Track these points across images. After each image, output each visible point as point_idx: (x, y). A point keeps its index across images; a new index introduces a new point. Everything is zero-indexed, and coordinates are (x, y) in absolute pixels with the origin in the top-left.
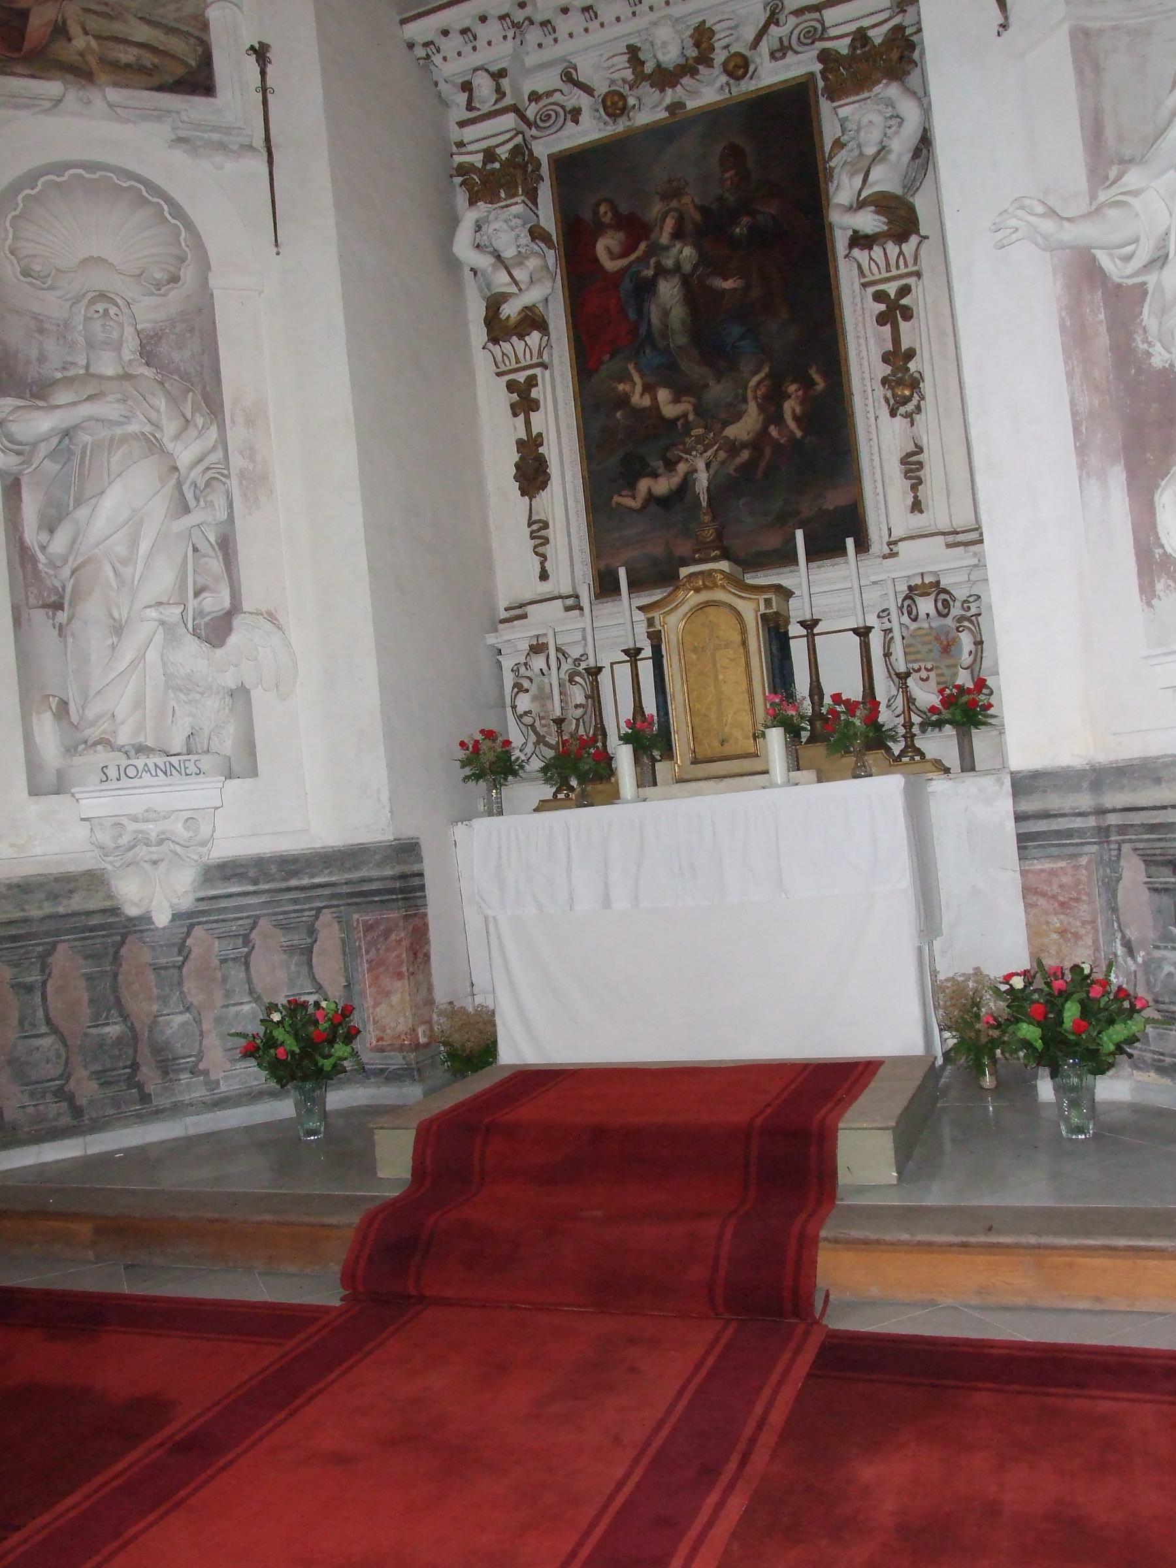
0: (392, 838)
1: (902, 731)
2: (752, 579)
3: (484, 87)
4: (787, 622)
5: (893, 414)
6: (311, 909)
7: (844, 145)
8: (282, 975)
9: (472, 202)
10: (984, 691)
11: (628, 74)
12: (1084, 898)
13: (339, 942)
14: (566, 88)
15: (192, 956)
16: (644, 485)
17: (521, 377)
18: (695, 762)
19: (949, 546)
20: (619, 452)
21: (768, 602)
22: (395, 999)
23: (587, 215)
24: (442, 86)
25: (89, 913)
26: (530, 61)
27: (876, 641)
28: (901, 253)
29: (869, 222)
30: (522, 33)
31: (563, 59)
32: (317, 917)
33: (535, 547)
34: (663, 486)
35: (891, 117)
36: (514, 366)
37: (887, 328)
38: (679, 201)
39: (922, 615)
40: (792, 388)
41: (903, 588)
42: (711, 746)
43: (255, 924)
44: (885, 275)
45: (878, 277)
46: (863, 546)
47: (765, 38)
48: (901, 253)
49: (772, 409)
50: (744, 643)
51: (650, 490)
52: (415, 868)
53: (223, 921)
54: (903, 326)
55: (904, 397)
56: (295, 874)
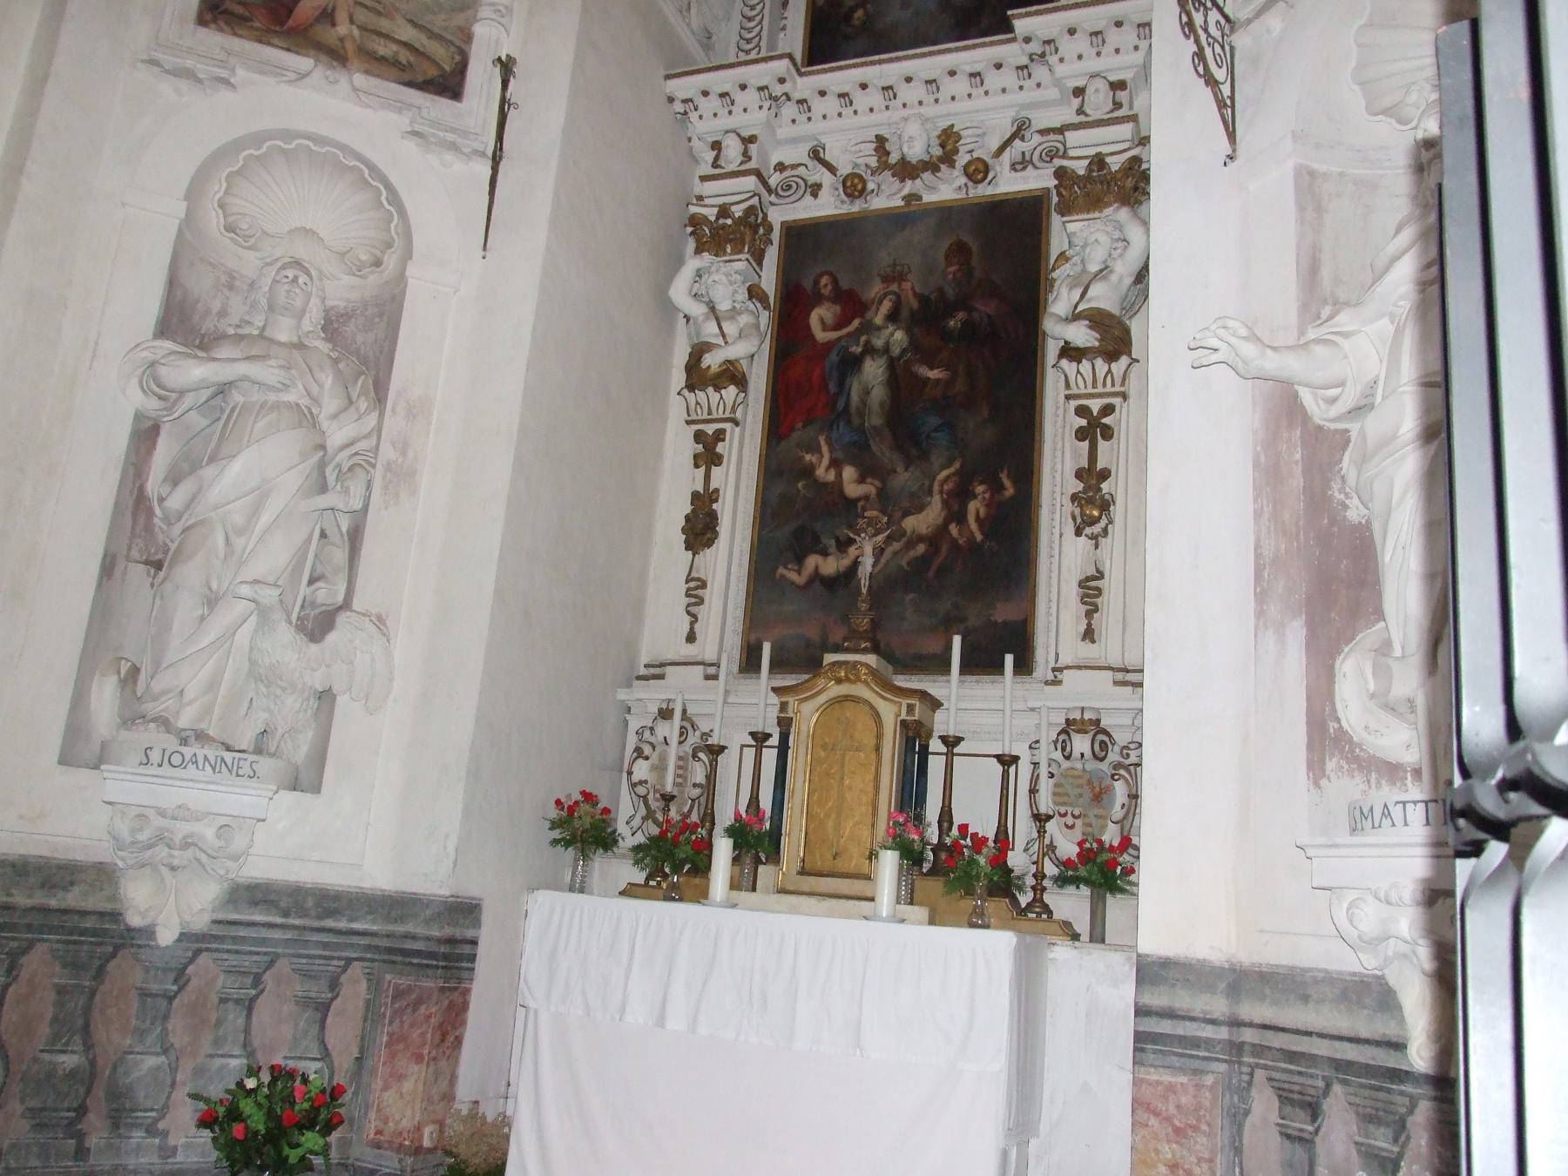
0: (447, 893)
1: (1030, 881)
2: (902, 681)
3: (733, 148)
4: (930, 735)
5: (1078, 533)
6: (339, 958)
7: (1067, 259)
8: (287, 1030)
9: (698, 251)
10: (1131, 851)
12: (1204, 1127)
13: (361, 1004)
14: (810, 163)
15: (190, 987)
16: (812, 561)
17: (710, 429)
18: (803, 872)
19: (1116, 683)
20: (795, 521)
21: (910, 708)
22: (408, 1086)
23: (808, 284)
24: (695, 143)
25: (84, 913)
26: (782, 133)
27: (1024, 768)
28: (1109, 371)
29: (1081, 335)
30: (779, 107)
32: (344, 970)
34: (831, 566)
36: (706, 416)
39: (1076, 754)
40: (980, 489)
42: (822, 860)
43: (272, 963)
46: (1024, 666)
48: (1109, 371)
50: (878, 749)
52: (470, 934)
53: (237, 952)
54: (1102, 445)
55: (1091, 516)
56: (330, 913)
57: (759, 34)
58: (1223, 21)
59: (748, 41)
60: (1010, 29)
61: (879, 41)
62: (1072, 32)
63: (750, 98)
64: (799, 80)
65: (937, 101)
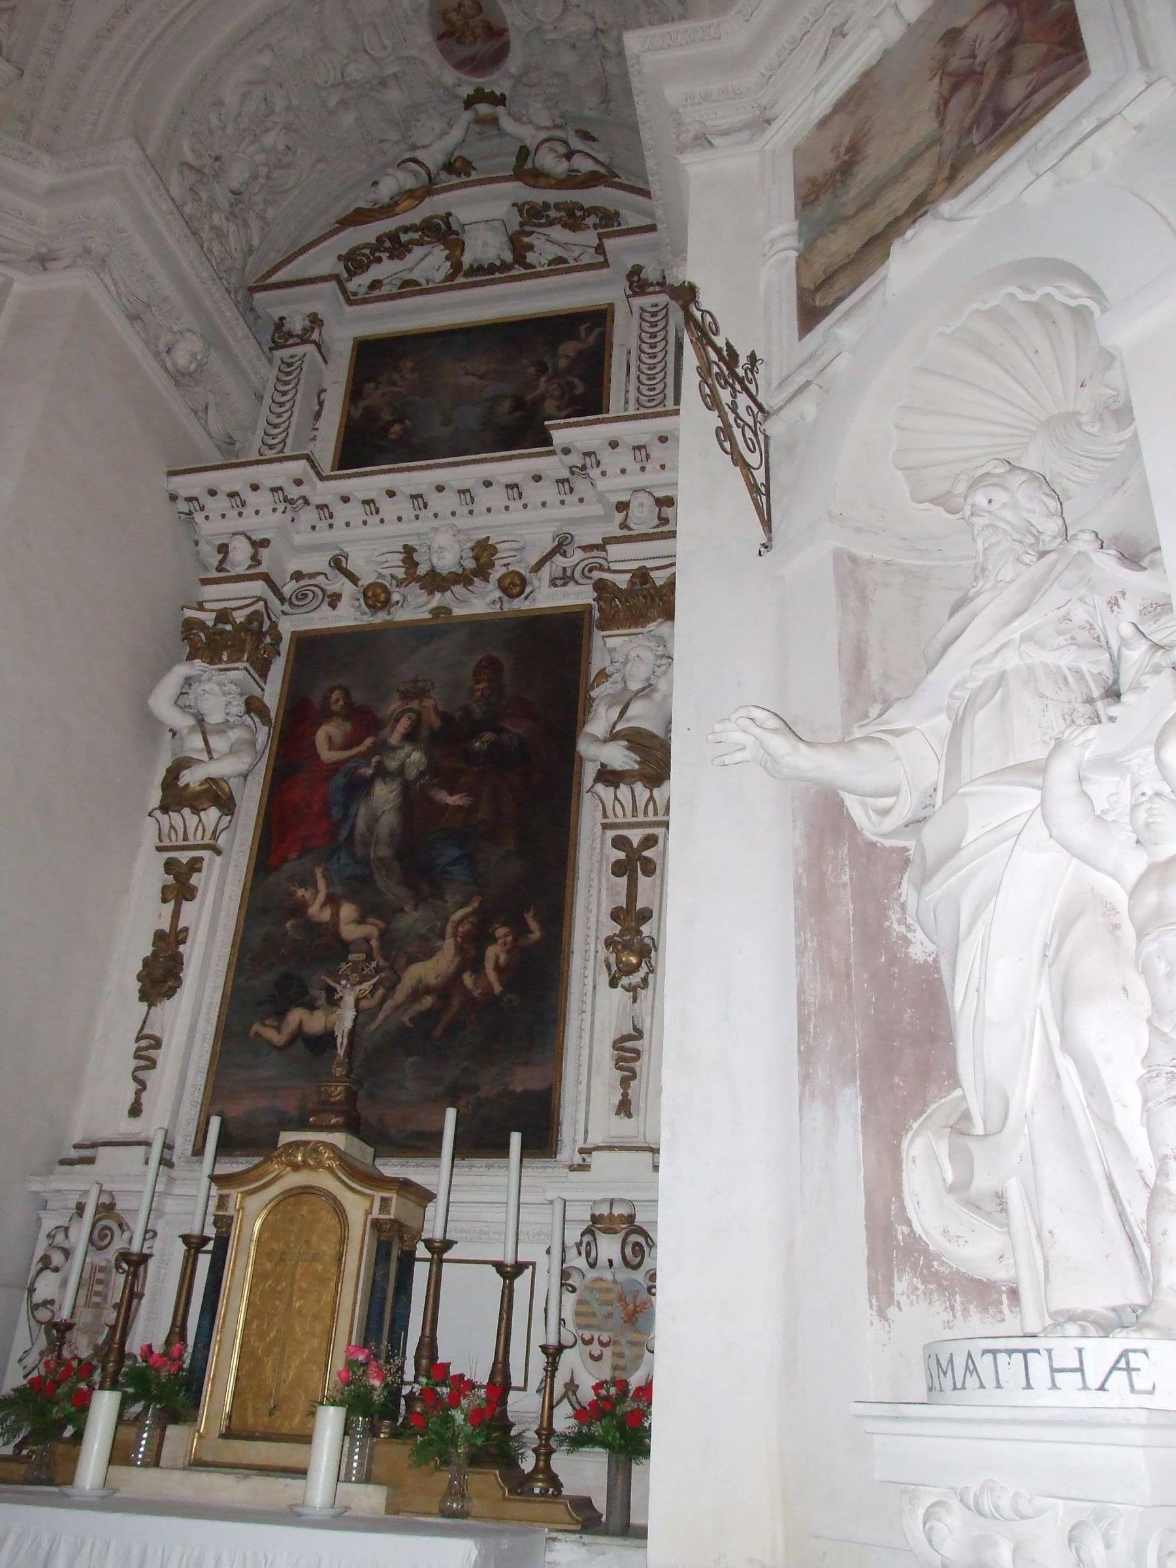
2: (391, 1168)
3: (241, 552)
5: (613, 983)
7: (607, 676)
11: (400, 573)
14: (331, 573)
16: (296, 1016)
17: (184, 857)
18: (228, 1434)
23: (317, 699)
24: (204, 547)
28: (651, 798)
29: (619, 757)
31: (335, 545)
33: (137, 1069)
35: (662, 656)
36: (181, 843)
38: (421, 702)
39: (603, 1260)
40: (501, 932)
41: (581, 1214)
45: (621, 820)
47: (548, 564)
48: (651, 798)
49: (472, 953)
51: (301, 1024)
54: (643, 881)
55: (629, 964)
57: (284, 441)
58: (756, 410)
59: (271, 447)
60: (548, 441)
61: (411, 449)
62: (614, 445)
63: (262, 499)
64: (320, 484)
65: (471, 512)
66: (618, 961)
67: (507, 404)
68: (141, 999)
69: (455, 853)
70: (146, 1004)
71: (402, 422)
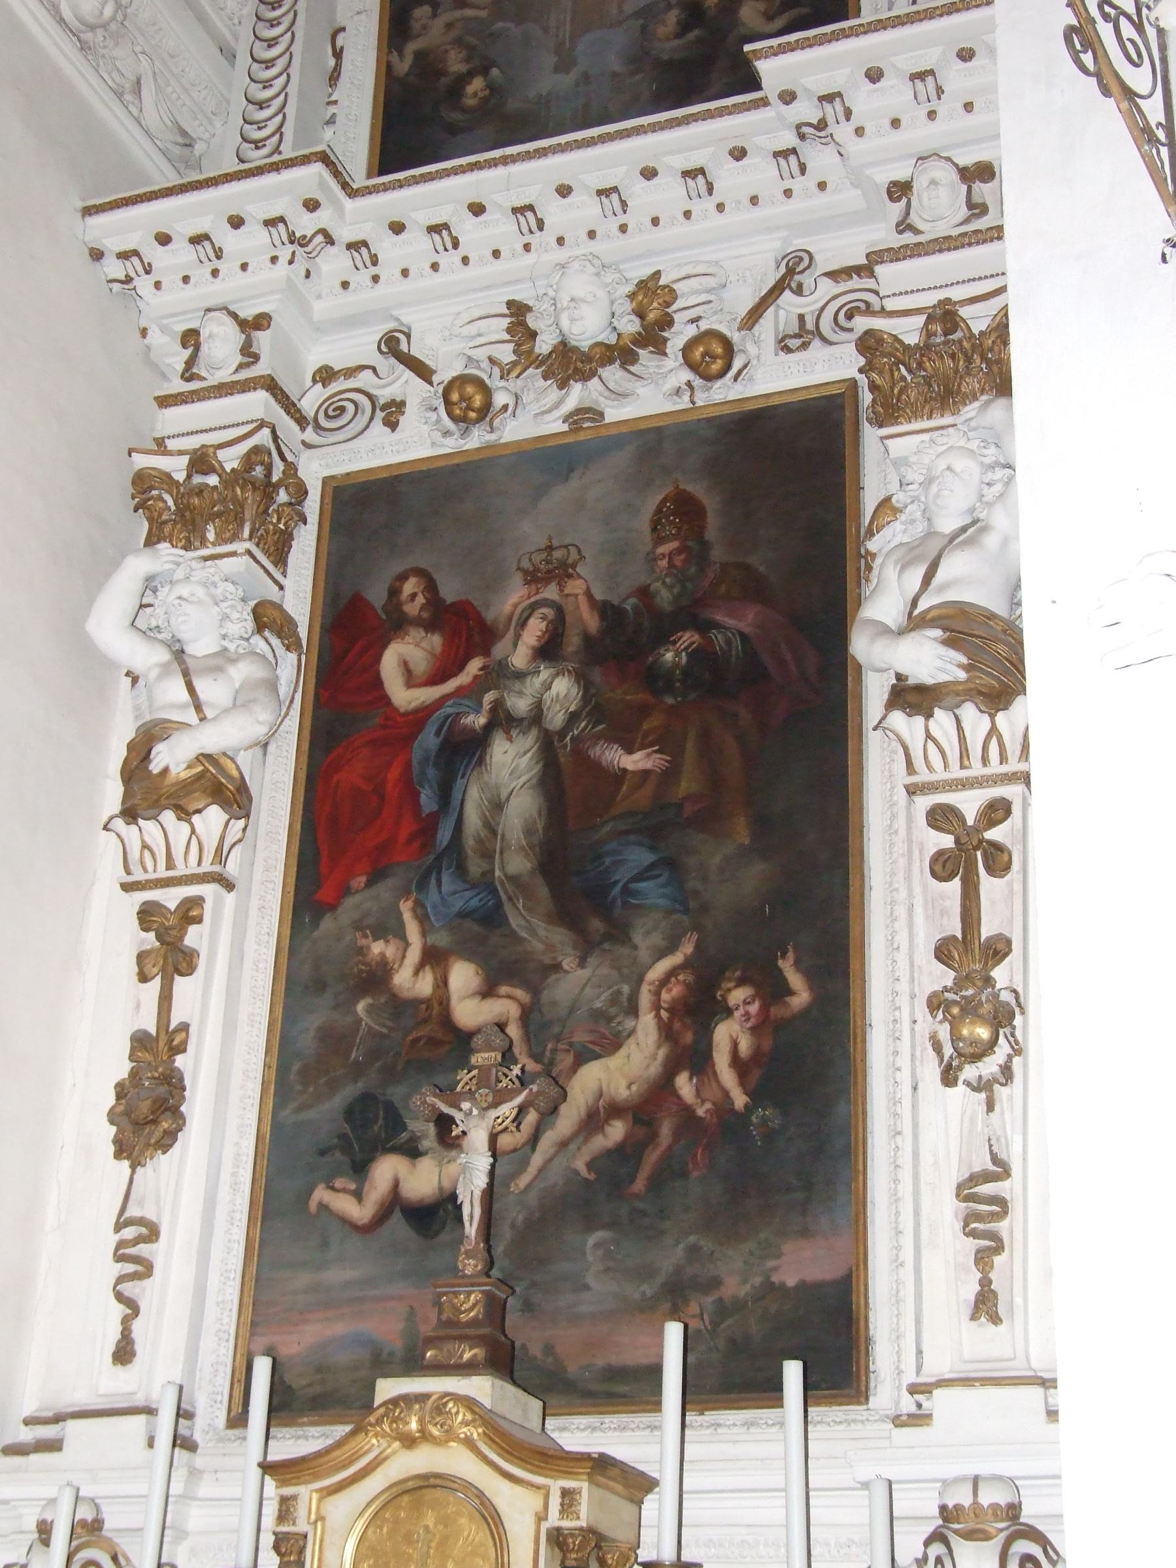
5: (949, 1077)
7: (896, 511)
11: (506, 354)
14: (386, 364)
16: (387, 1170)
17: (170, 898)
20: (351, 1085)
23: (377, 595)
24: (155, 337)
26: (320, 309)
28: (993, 730)
29: (929, 660)
33: (121, 1279)
36: (162, 873)
37: (954, 886)
40: (738, 996)
44: (956, 773)
45: (940, 775)
47: (771, 310)
48: (993, 730)
51: (396, 1184)
55: (974, 1042)
59: (258, 144)
60: (752, 82)
62: (874, 75)
63: (253, 241)
64: (349, 204)
65: (623, 228)
66: (955, 1037)
67: (673, 17)
68: (118, 1155)
69: (647, 858)
70: (126, 1164)
71: (484, 71)
